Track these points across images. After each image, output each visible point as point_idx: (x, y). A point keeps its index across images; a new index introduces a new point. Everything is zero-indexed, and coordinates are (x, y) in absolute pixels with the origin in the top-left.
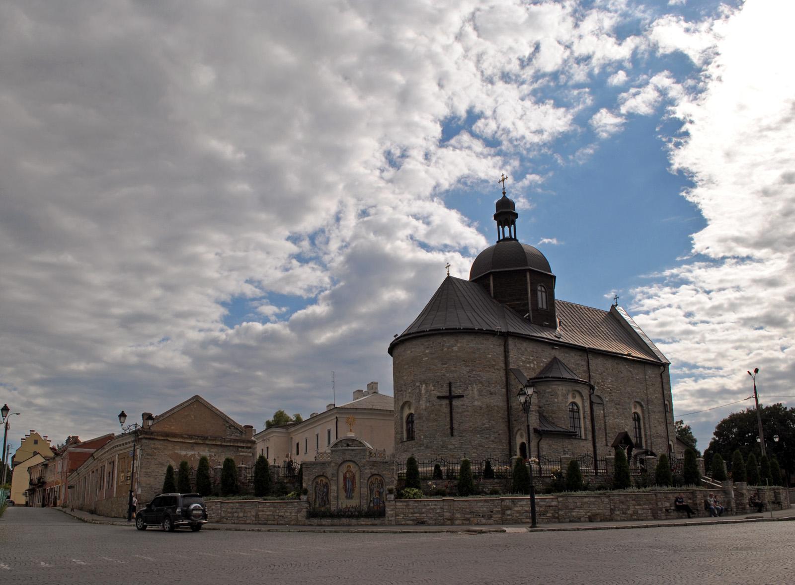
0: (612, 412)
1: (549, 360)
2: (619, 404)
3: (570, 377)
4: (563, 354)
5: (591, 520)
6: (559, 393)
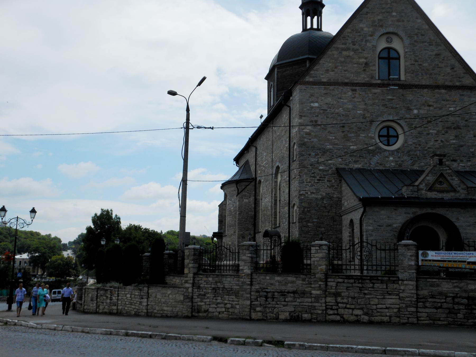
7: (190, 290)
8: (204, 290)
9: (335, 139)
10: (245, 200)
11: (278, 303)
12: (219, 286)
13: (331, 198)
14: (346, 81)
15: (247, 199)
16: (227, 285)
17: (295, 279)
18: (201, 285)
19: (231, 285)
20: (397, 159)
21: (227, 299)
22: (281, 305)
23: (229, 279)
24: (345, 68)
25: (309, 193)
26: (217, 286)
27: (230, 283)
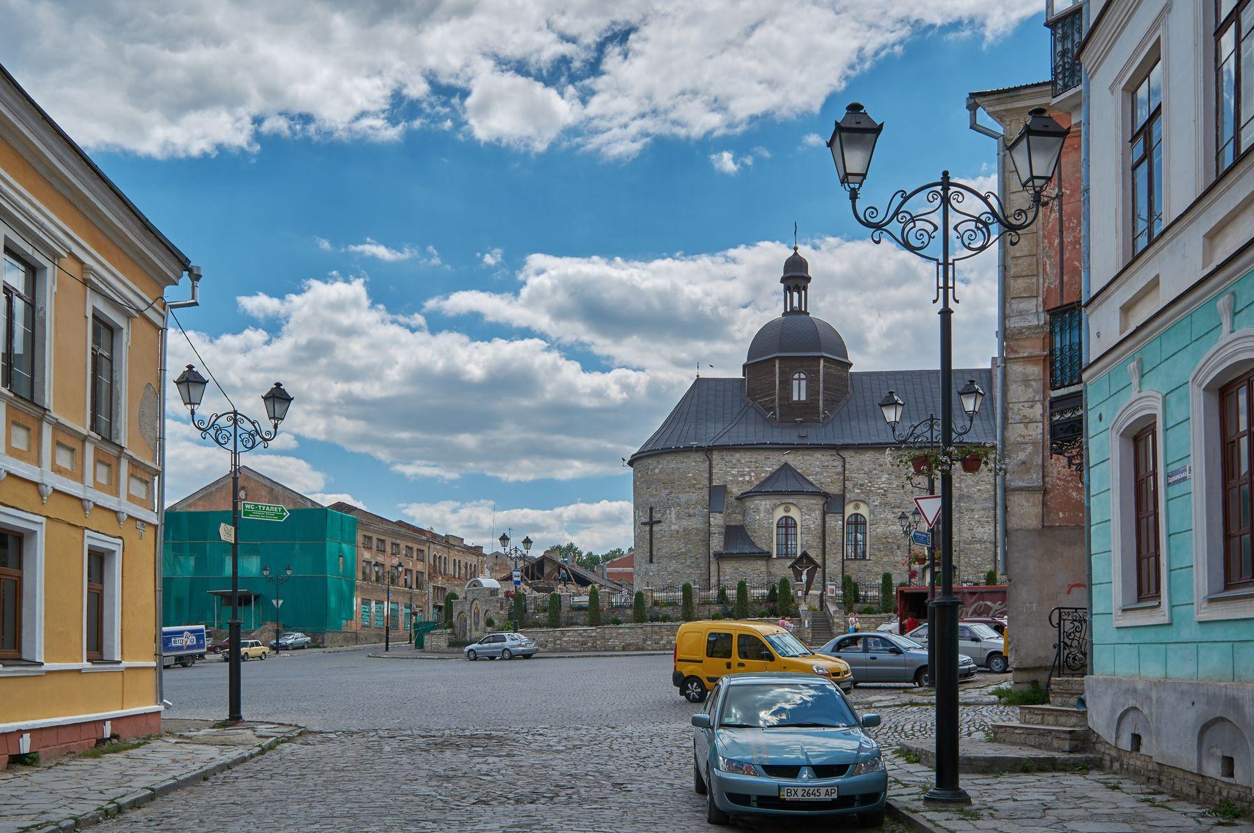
0: (885, 519)
1: (776, 467)
3: (798, 488)
5: (624, 649)
6: (762, 508)
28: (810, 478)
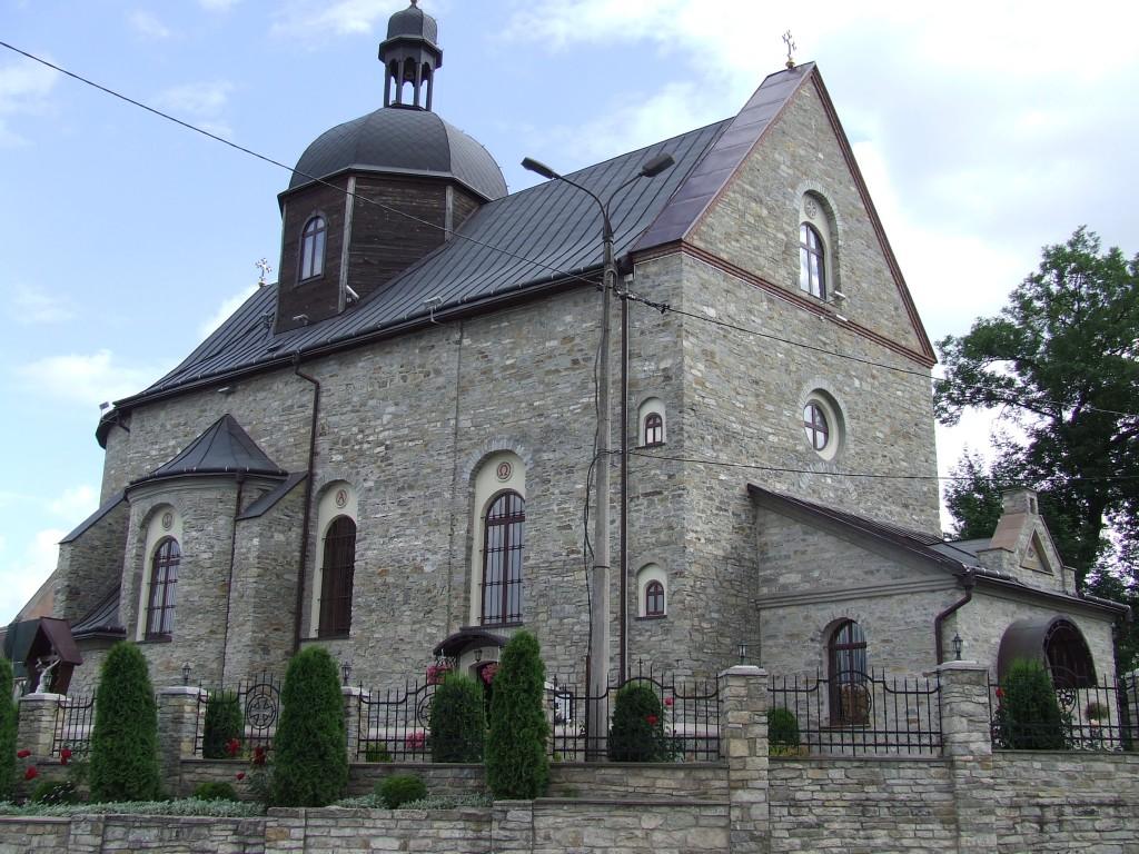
0: (384, 522)
2: (411, 487)
4: (251, 398)
7: (759, 811)
8: (817, 811)
9: (745, 409)
10: (276, 535)
11: (1076, 835)
12: (873, 796)
13: (740, 560)
14: (759, 273)
15: (283, 532)
16: (906, 789)
17: (1111, 767)
18: (799, 795)
19: (920, 789)
20: (837, 485)
21: (912, 834)
22: (1084, 839)
23: (909, 773)
24: (755, 242)
25: (703, 541)
26: (863, 796)
27: (918, 784)
28: (262, 443)
